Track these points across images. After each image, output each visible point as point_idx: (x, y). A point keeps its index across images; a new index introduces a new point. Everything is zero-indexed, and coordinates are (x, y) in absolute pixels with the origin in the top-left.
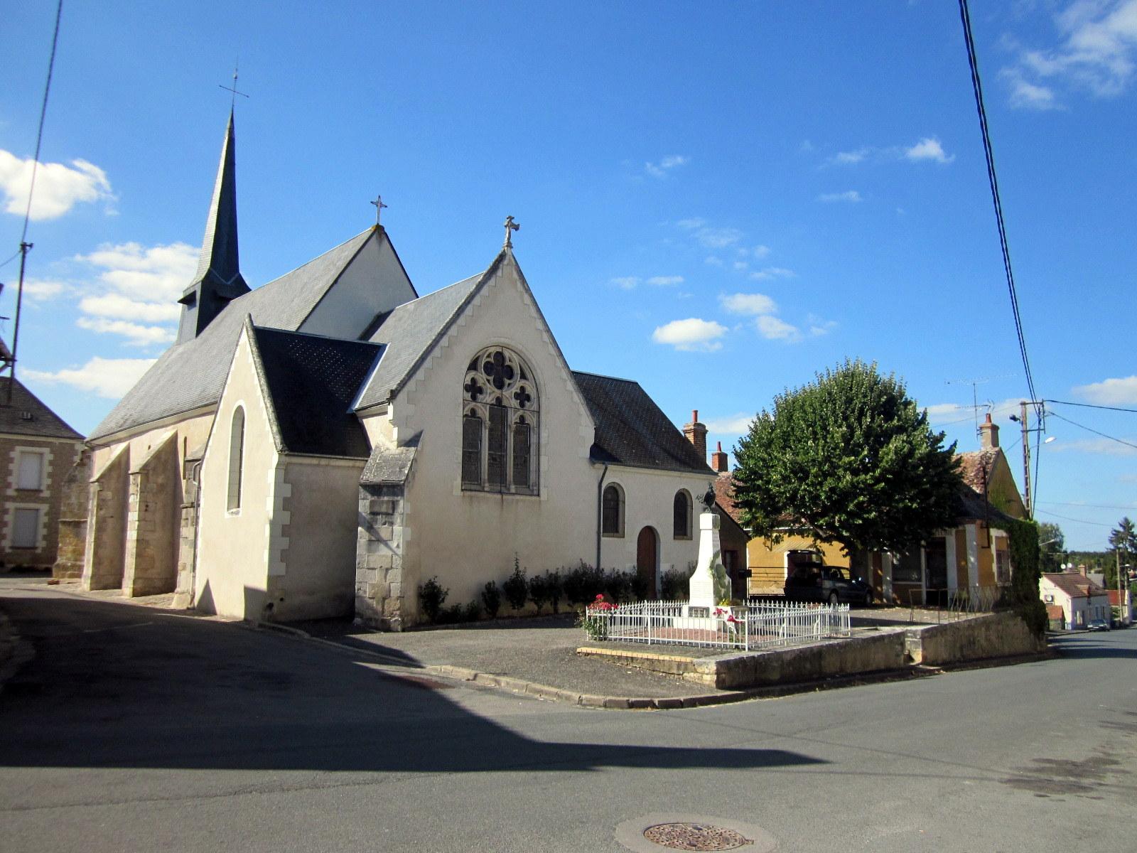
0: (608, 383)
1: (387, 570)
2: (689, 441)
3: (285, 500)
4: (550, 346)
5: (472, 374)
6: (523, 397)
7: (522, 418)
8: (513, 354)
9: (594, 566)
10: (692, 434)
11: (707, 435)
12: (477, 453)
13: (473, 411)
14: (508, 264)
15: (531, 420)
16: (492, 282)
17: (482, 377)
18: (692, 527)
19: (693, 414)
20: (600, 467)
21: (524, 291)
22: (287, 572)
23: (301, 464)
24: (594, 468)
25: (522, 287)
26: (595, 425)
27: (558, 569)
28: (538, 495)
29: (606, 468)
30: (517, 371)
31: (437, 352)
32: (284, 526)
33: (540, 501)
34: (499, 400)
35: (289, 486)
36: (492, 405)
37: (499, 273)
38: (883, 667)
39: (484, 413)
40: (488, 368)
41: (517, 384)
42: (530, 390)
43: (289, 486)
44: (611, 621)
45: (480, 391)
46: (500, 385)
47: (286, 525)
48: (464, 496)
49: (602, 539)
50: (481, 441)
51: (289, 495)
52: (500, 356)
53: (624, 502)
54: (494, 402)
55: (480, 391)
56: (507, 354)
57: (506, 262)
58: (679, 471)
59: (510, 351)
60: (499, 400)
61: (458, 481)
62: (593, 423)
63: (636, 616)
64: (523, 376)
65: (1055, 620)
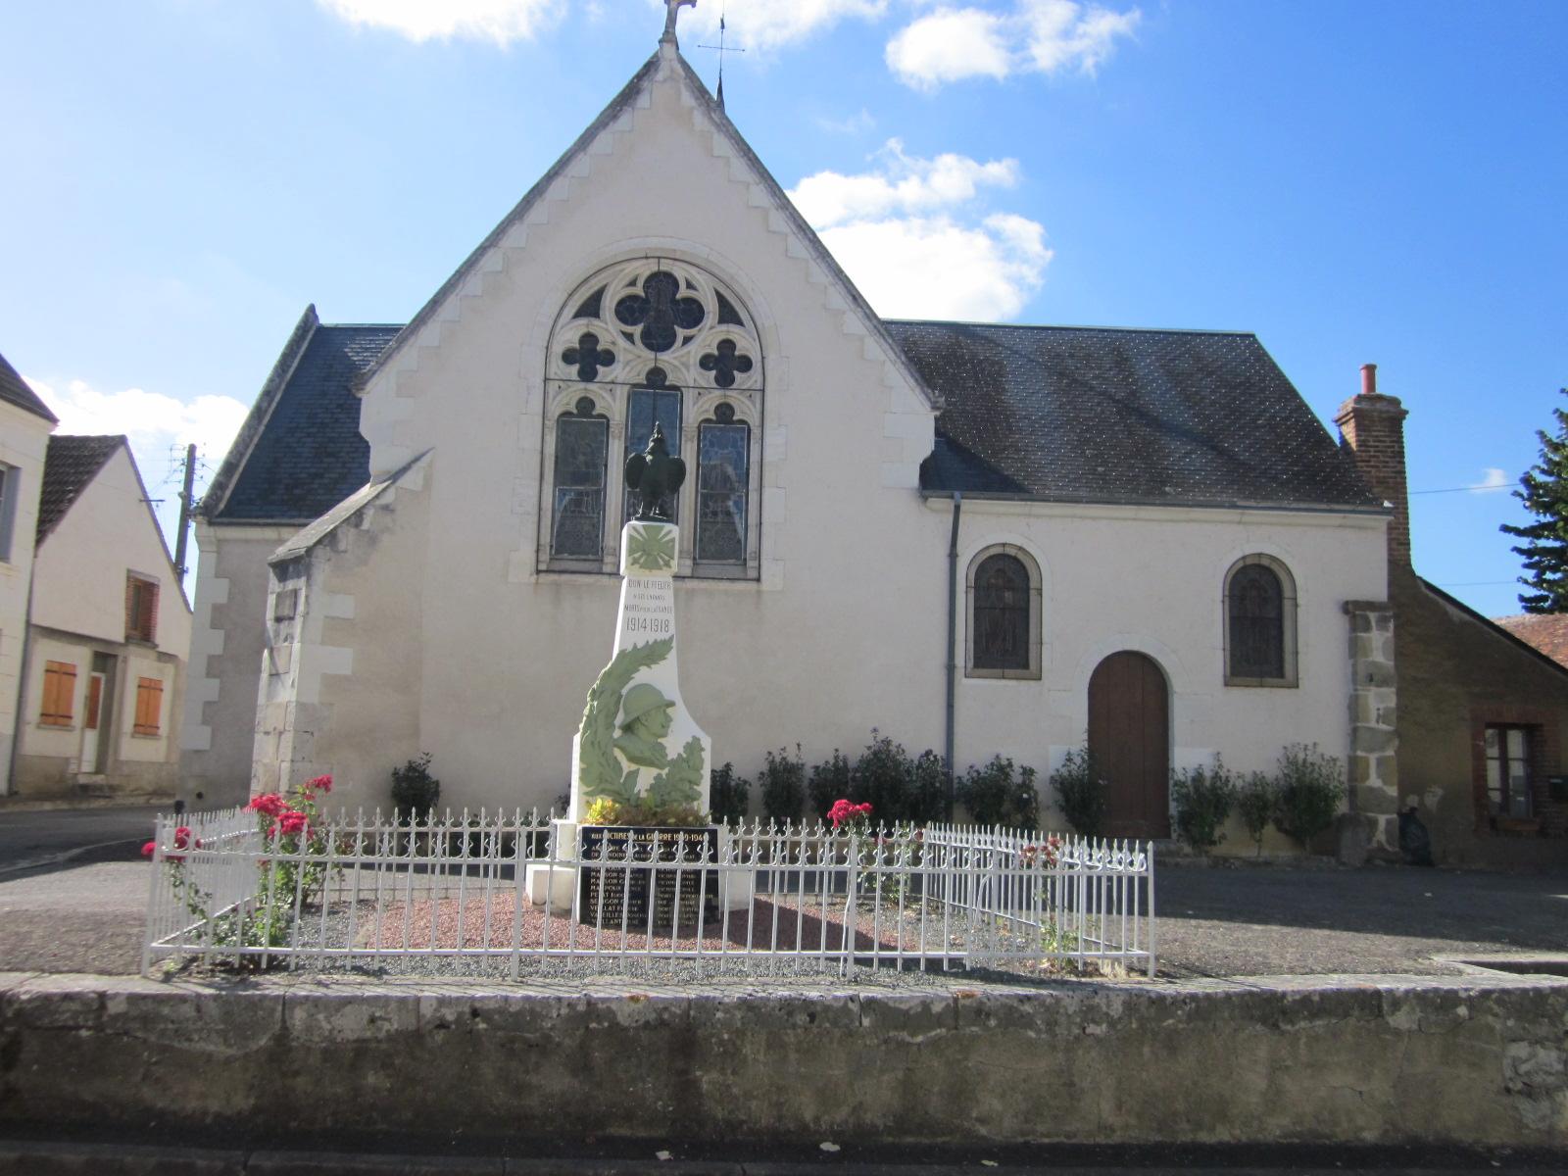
0: (1133, 340)
1: (281, 733)
2: (1330, 438)
3: (217, 609)
4: (792, 239)
5: (583, 326)
6: (726, 364)
7: (725, 412)
8: (693, 271)
9: (939, 750)
10: (1352, 423)
11: (1405, 423)
12: (598, 492)
13: (586, 405)
14: (665, 81)
15: (745, 409)
16: (624, 120)
17: (608, 330)
18: (1297, 653)
19: (1363, 374)
20: (942, 505)
21: (713, 129)
22: (212, 746)
23: (247, 541)
24: (926, 507)
25: (706, 121)
26: (934, 408)
27: (784, 749)
28: (758, 580)
29: (957, 508)
30: (711, 307)
31: (473, 284)
32: (211, 658)
33: (759, 593)
34: (656, 376)
35: (225, 583)
36: (635, 386)
37: (643, 101)
38: (1370, 1136)
39: (614, 406)
40: (628, 310)
41: (708, 337)
42: (745, 344)
43: (225, 583)
44: (1045, 885)
45: (608, 358)
46: (658, 340)
47: (213, 656)
48: (537, 583)
49: (966, 685)
50: (606, 466)
51: (223, 599)
52: (662, 282)
53: (1040, 591)
54: (642, 380)
55: (608, 358)
56: (680, 273)
57: (660, 76)
58: (1234, 506)
59: (684, 265)
60: (656, 376)
61: (526, 554)
62: (928, 406)
63: (1014, 873)
64: (728, 314)
65: (89, 762)
